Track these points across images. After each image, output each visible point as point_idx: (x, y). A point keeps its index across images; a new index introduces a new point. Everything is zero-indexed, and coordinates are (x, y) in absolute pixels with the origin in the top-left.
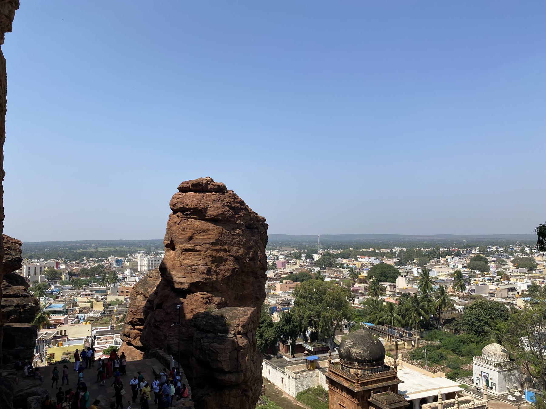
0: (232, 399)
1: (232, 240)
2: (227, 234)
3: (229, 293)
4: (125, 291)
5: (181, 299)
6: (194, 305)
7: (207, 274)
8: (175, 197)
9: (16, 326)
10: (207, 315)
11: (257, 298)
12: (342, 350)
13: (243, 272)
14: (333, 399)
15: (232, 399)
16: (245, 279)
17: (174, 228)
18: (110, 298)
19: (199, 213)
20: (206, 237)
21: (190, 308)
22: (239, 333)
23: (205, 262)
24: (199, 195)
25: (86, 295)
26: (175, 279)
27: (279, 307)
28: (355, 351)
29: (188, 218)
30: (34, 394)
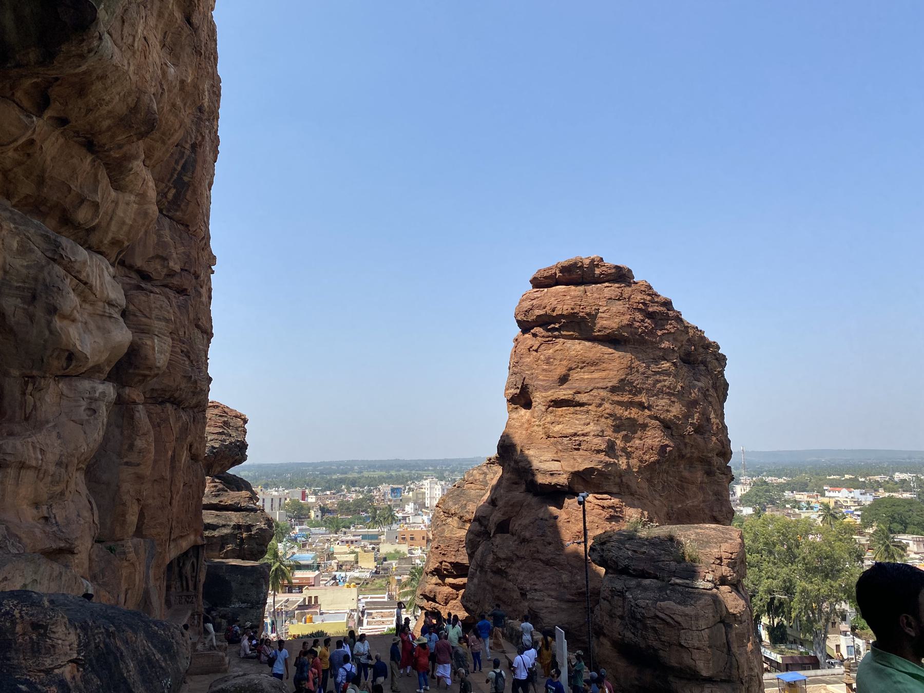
1: (654, 385)
2: (641, 370)
3: (657, 503)
4: (408, 537)
5: (553, 509)
6: (579, 523)
13: (682, 456)
16: (686, 474)
17: (528, 360)
18: (386, 548)
19: (578, 325)
22: (723, 581)
23: (599, 428)
25: (347, 542)
26: (536, 464)
29: (556, 337)
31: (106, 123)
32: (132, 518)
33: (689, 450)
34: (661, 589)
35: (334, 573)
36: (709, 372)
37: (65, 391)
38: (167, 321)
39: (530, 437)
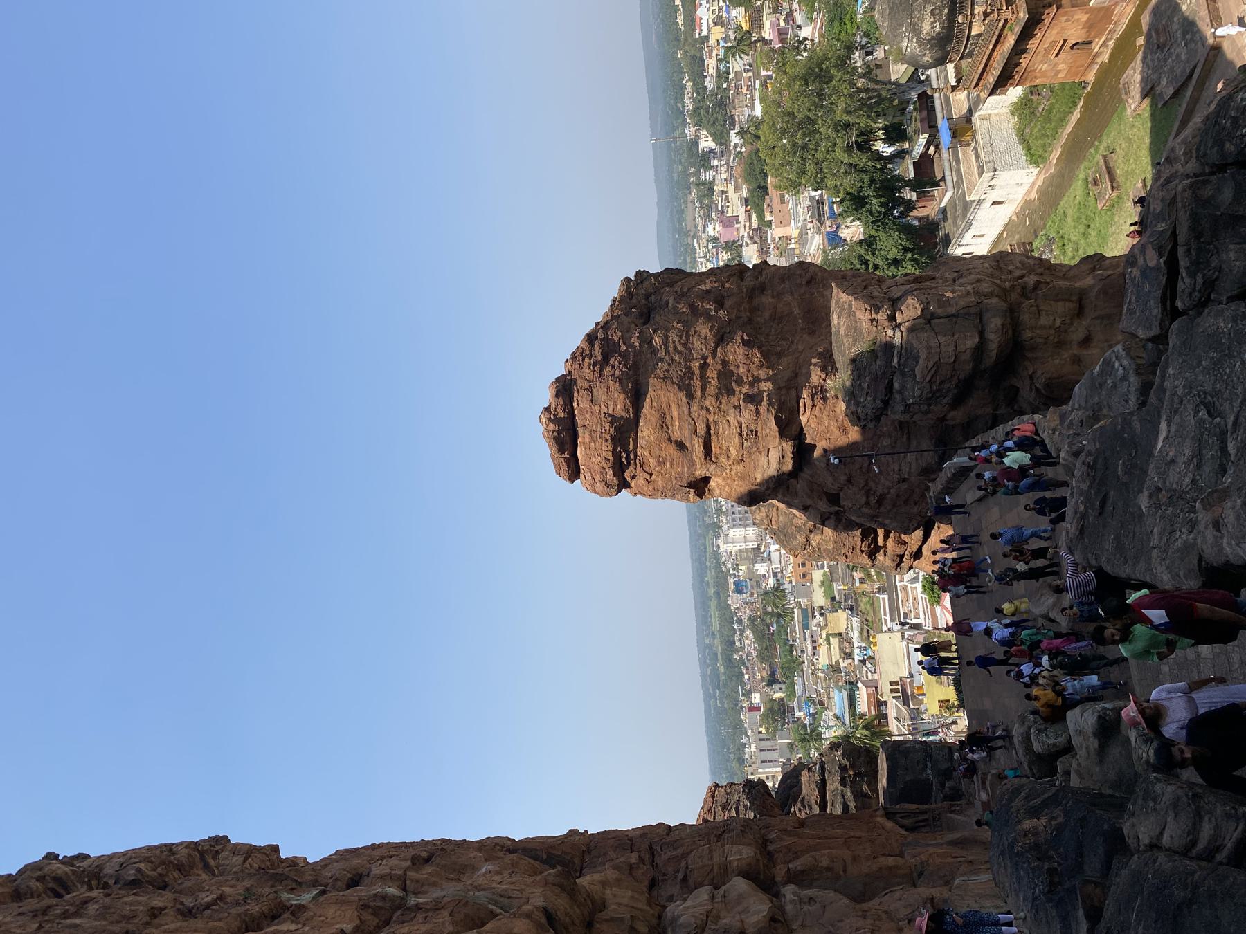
0: (1043, 321)
1: (680, 353)
3: (800, 348)
5: (816, 454)
6: (829, 425)
7: (760, 403)
8: (592, 486)
9: (885, 781)
10: (851, 396)
11: (809, 282)
12: (927, 59)
13: (750, 321)
14: (1043, 74)
15: (1043, 321)
16: (767, 315)
18: (819, 599)
19: (623, 434)
21: (836, 432)
22: (892, 318)
24: (583, 437)
25: (814, 648)
26: (772, 472)
27: (828, 226)
28: (929, 25)
29: (636, 455)
30: (1027, 739)
31: (578, 911)
32: (891, 861)
33: (742, 314)
34: (903, 374)
35: (856, 662)
36: (656, 291)
37: (799, 923)
38: (711, 850)
39: (742, 478)
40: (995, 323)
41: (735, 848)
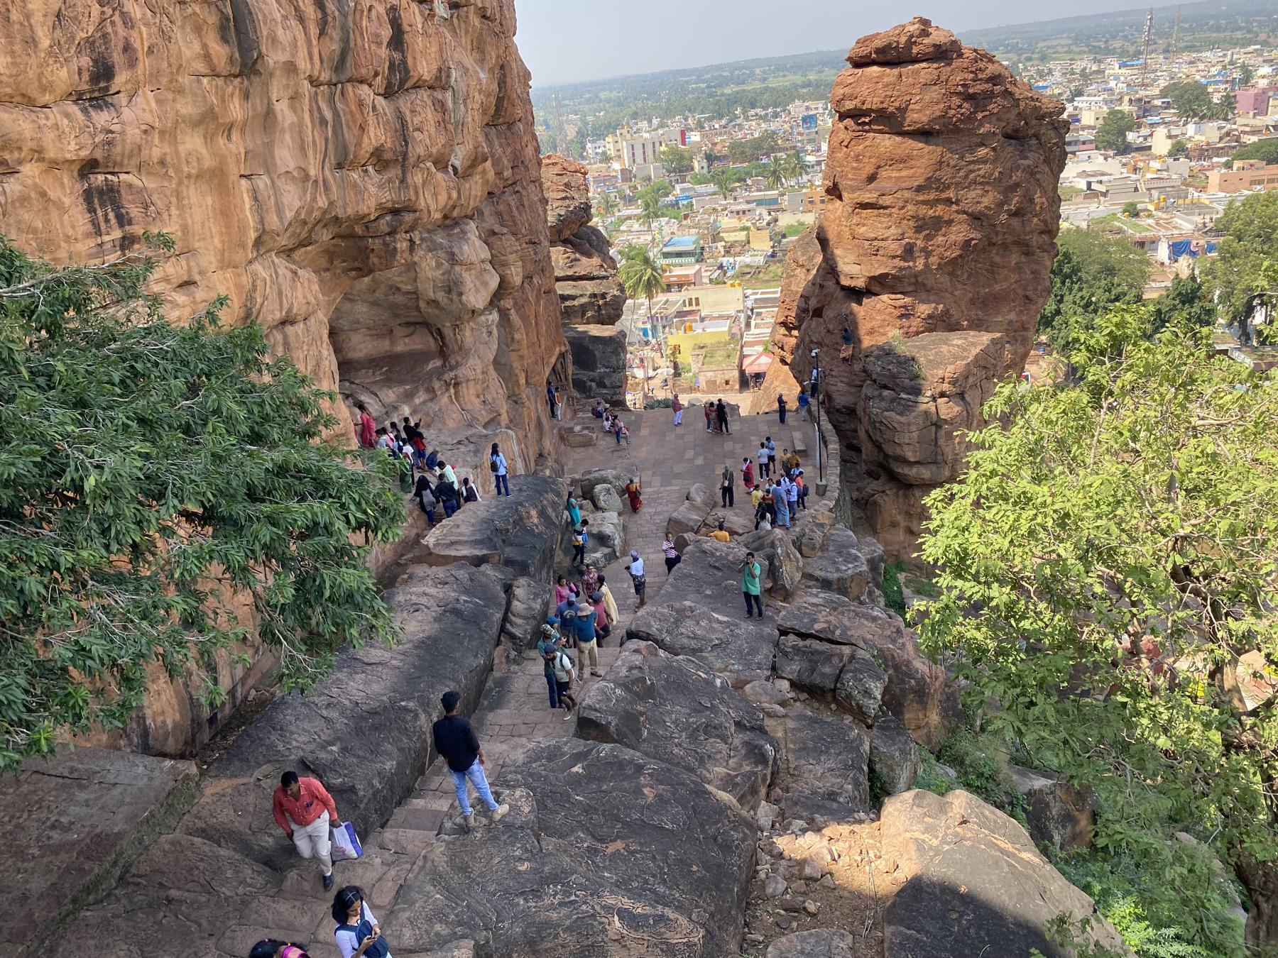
1: (966, 177)
2: (952, 163)
3: (956, 293)
5: (854, 305)
7: (903, 258)
11: (1027, 297)
13: (992, 244)
16: (997, 259)
18: (786, 220)
19: (887, 120)
20: (904, 173)
22: (942, 395)
23: (900, 231)
25: (738, 213)
27: (1200, 241)
29: (867, 131)
32: (522, 381)
33: (1000, 237)
34: (893, 400)
35: (721, 259)
38: (516, 252)
40: (926, 473)
41: (520, 270)
